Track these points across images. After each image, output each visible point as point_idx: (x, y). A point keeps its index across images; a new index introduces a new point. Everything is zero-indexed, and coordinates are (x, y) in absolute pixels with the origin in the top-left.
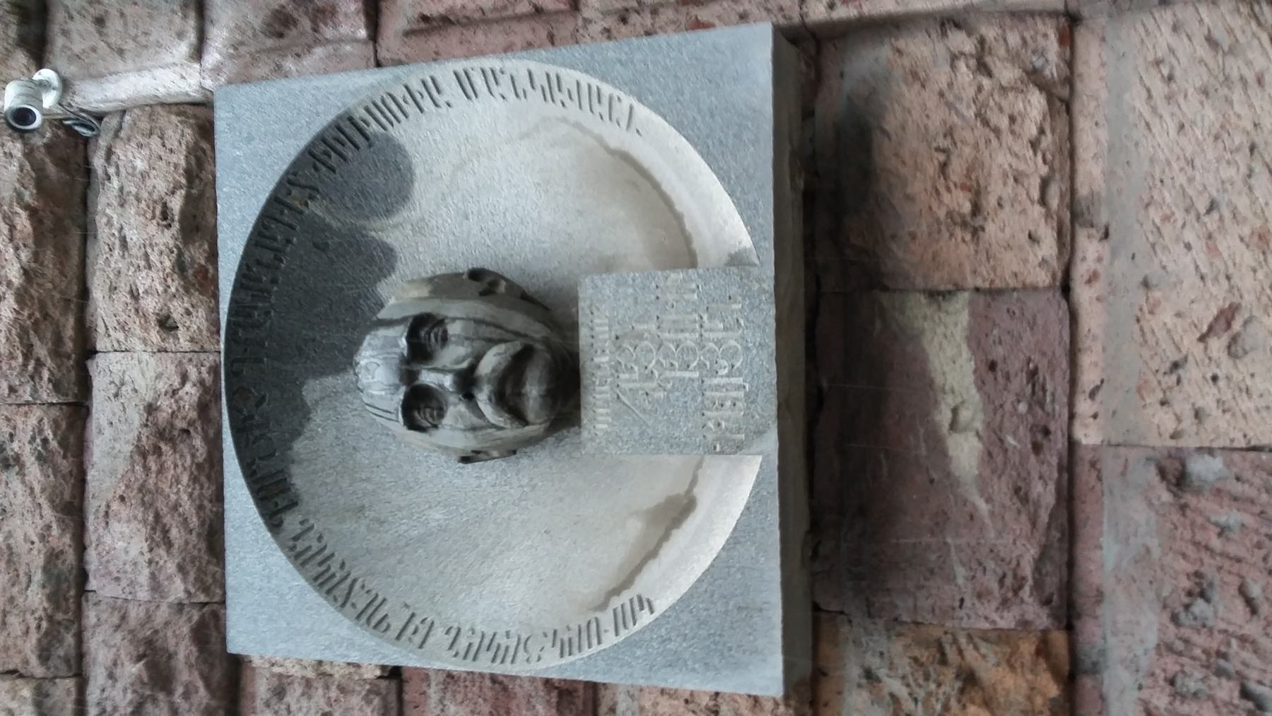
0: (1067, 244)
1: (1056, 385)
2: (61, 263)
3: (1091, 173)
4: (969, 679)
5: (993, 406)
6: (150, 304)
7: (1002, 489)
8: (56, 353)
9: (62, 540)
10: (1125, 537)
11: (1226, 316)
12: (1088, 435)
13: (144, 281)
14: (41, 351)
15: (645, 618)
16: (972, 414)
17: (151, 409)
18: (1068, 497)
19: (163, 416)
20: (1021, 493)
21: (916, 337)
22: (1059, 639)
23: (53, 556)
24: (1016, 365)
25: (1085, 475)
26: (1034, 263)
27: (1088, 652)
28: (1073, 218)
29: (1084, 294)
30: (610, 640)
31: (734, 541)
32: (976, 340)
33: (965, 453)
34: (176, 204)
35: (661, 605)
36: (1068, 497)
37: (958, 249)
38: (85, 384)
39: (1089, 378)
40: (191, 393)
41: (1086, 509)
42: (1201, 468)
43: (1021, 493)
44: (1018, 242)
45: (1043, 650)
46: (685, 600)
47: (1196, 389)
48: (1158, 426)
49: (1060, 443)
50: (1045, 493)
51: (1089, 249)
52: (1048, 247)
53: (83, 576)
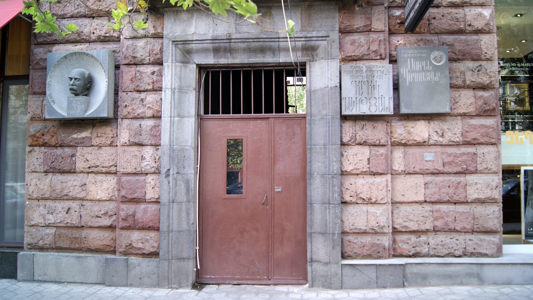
0: (97, 146)
1: (83, 145)
2: (105, 14)
3: (104, 148)
4: (53, 136)
5: (80, 138)
6: (95, 31)
7: (71, 139)
8: (92, 14)
9: (68, 15)
10: (68, 151)
11: (88, 160)
12: (78, 148)
13: (98, 31)
14: (91, 12)
15: (52, 104)
16: (79, 137)
17: (82, 32)
18: (72, 146)
19: (81, 34)
20: (71, 141)
21: (87, 131)
22: (58, 145)
23: (66, 14)
24: (84, 141)
25: (75, 148)
26: (94, 143)
27: (58, 148)
28: (100, 147)
29: (92, 148)
30: (50, 100)
31: (59, 113)
32: (86, 137)
33: (75, 136)
34: (107, 35)
35: (54, 106)
36: (72, 146)
37: (95, 135)
38: (89, 17)
39: (84, 148)
40: (85, 37)
41: (71, 148)
42: (74, 159)
43: (71, 141)
44: (96, 141)
45: (57, 144)
46: (54, 108)
47: (81, 158)
48: (78, 154)
49: (77, 145)
50: (71, 144)
51: (97, 148)
52: (96, 144)
53: (64, 18)
